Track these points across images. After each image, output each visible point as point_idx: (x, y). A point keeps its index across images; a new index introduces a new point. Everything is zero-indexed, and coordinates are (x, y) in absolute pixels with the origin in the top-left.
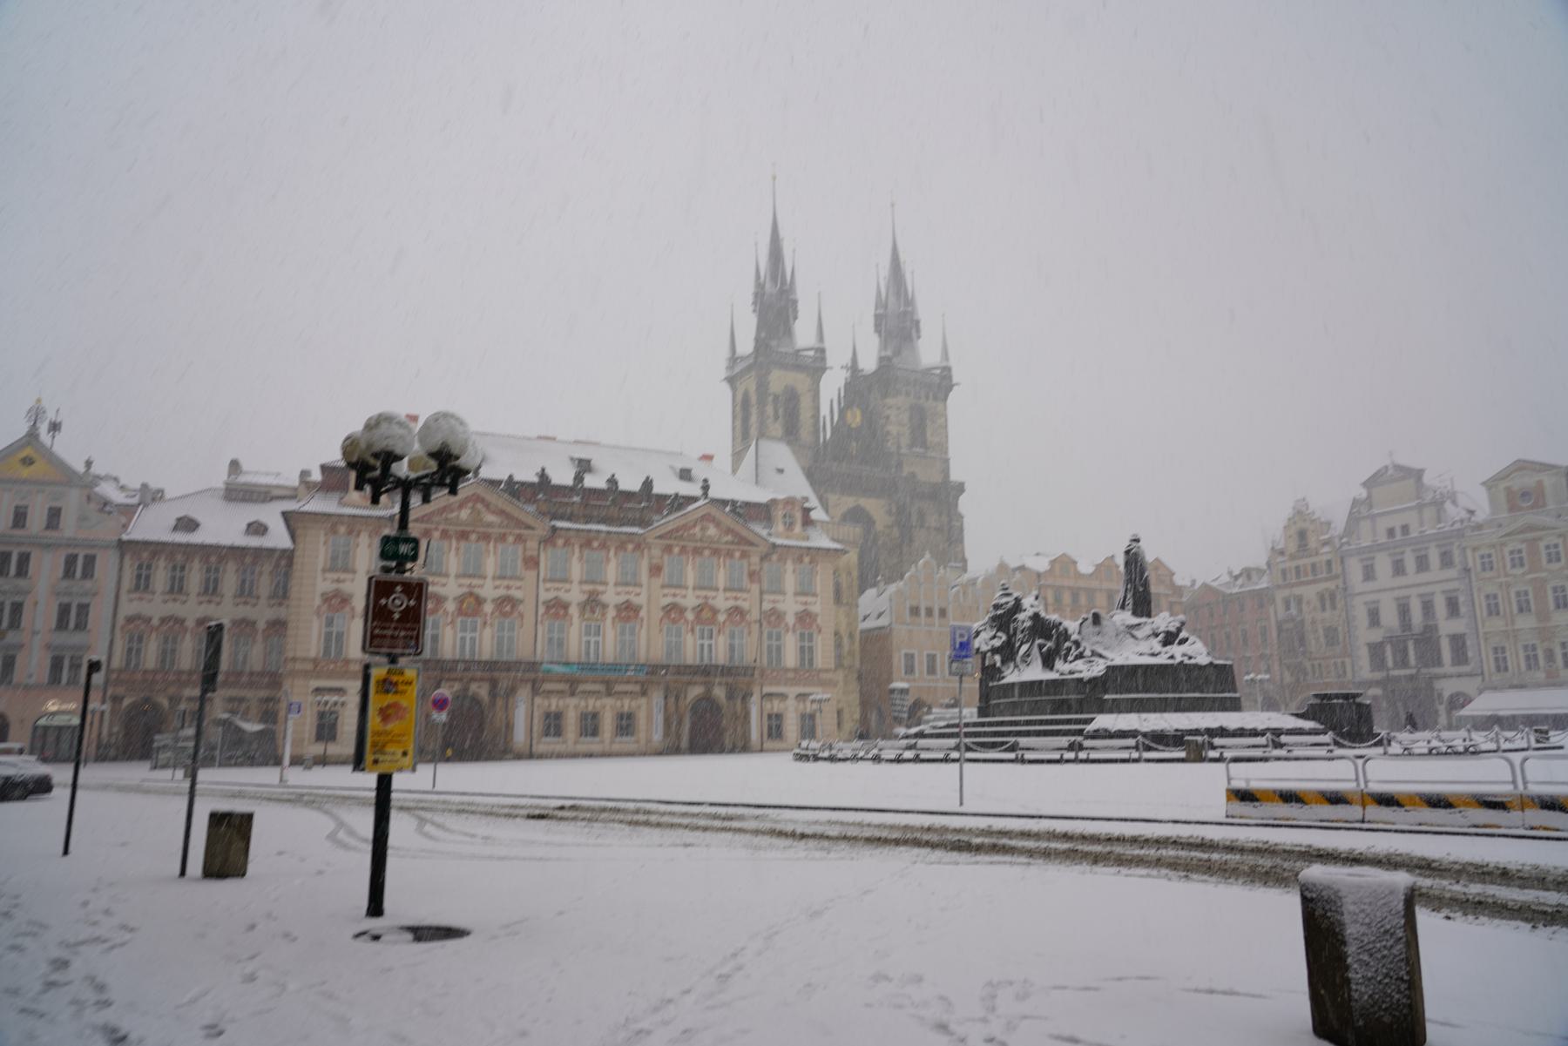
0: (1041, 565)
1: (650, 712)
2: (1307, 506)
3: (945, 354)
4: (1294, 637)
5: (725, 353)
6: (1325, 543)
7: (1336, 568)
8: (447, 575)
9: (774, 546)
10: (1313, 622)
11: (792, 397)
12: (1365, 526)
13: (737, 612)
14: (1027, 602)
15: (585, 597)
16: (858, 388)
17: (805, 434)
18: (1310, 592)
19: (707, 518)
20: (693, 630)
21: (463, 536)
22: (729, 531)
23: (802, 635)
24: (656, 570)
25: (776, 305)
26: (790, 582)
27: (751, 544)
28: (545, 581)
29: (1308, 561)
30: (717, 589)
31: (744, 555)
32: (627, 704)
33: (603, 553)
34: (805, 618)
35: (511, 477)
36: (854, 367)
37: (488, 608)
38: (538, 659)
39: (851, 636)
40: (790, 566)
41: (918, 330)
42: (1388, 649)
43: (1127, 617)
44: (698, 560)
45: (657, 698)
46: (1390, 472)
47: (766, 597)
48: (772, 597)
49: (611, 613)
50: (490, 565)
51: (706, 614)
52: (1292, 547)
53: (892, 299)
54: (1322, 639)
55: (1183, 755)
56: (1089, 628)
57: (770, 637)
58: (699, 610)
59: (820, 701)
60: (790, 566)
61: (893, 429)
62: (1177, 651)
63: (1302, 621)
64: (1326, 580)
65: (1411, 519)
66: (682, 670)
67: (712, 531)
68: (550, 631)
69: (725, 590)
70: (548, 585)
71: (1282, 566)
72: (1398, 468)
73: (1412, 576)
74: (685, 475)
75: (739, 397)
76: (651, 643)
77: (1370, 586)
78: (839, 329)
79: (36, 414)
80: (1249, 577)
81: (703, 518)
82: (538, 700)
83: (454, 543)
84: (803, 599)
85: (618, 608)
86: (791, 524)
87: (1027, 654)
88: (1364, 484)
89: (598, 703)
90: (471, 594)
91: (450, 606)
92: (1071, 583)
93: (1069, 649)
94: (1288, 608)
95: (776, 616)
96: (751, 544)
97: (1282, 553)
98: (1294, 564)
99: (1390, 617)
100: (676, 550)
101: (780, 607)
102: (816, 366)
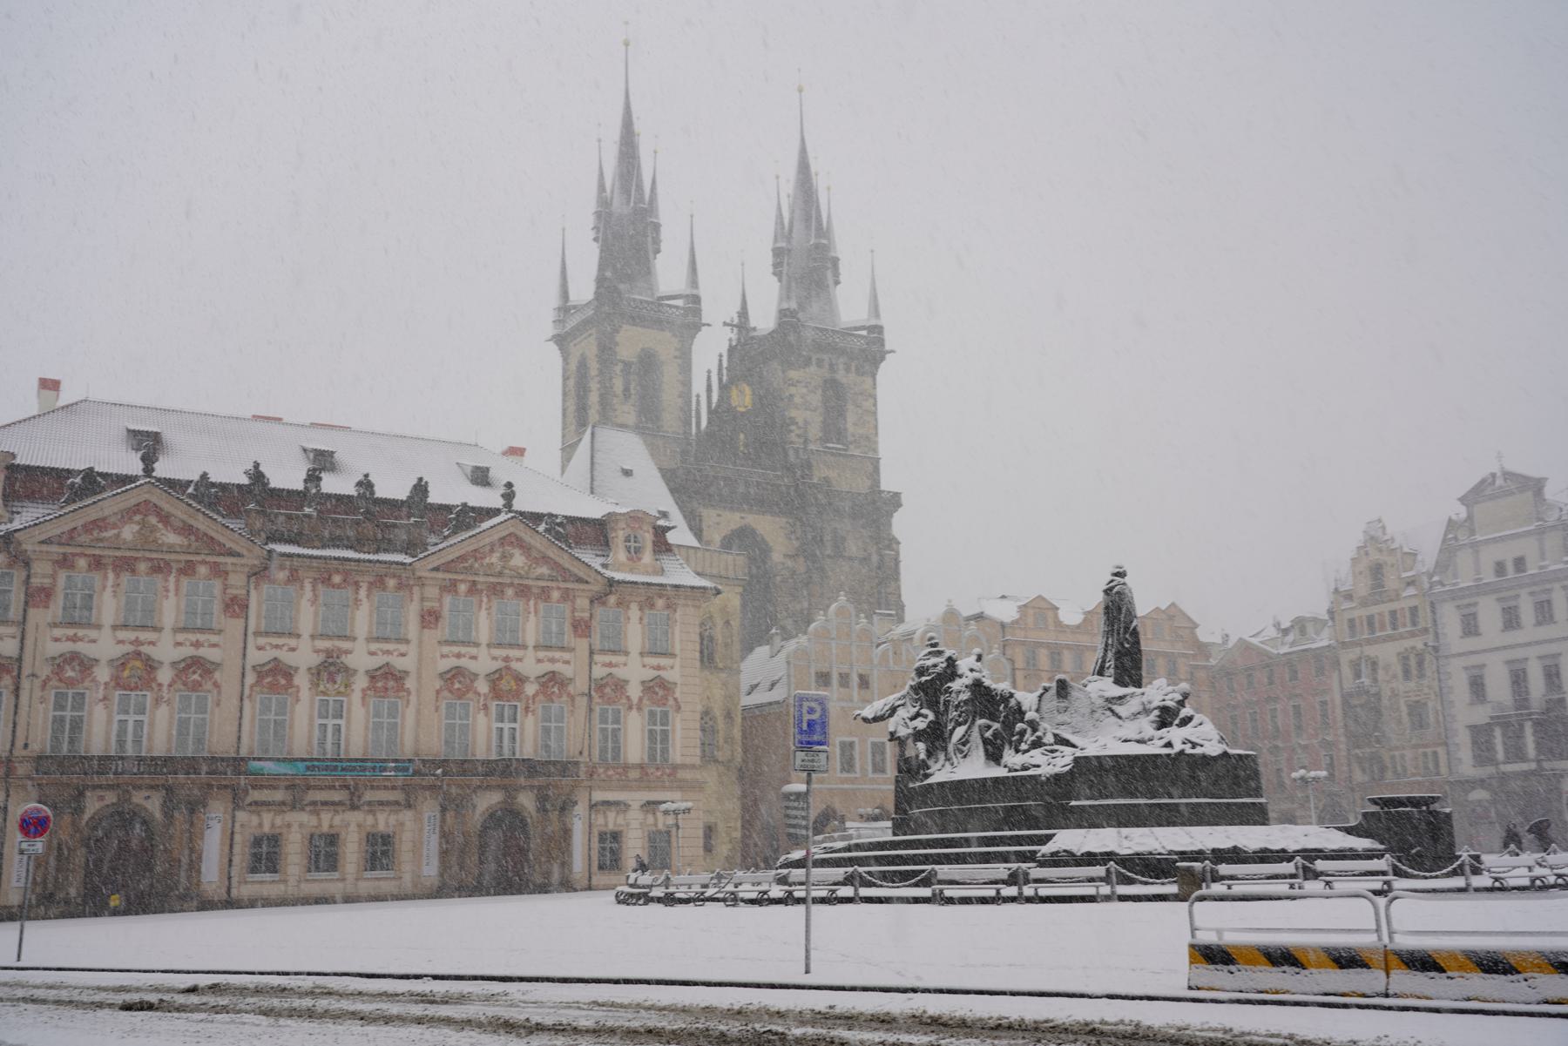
0: (1006, 612)
1: (419, 835)
3: (875, 310)
4: (1365, 713)
5: (554, 301)
6: (1411, 583)
7: (1425, 620)
8: (99, 627)
9: (611, 582)
10: (1394, 694)
11: (648, 363)
12: (1464, 560)
13: (552, 681)
14: (964, 665)
15: (320, 658)
16: (749, 354)
17: (670, 421)
18: (1387, 653)
20: (486, 707)
21: (125, 565)
22: (545, 559)
23: (652, 714)
24: (430, 618)
25: (628, 234)
26: (635, 636)
27: (580, 580)
28: (257, 634)
29: (1385, 608)
30: (525, 647)
31: (567, 596)
32: (383, 822)
33: (349, 592)
34: (658, 688)
35: (204, 476)
36: (742, 323)
37: (165, 675)
38: (244, 753)
39: (729, 716)
40: (634, 612)
41: (836, 274)
42: (1498, 732)
43: (1107, 686)
45: (429, 809)
46: (1499, 482)
47: (597, 658)
48: (608, 658)
49: (361, 682)
50: (169, 612)
51: (505, 685)
52: (1363, 589)
53: (799, 227)
54: (1406, 719)
55: (1173, 889)
56: (1051, 702)
57: (604, 720)
58: (495, 679)
59: (676, 813)
60: (634, 612)
61: (799, 415)
62: (1176, 734)
63: (1378, 695)
64: (1412, 635)
65: (1528, 548)
66: (465, 767)
67: (518, 560)
68: (266, 708)
69: (536, 647)
70: (262, 641)
71: (1347, 616)
72: (1508, 475)
73: (1529, 630)
74: (481, 477)
75: (573, 366)
76: (421, 728)
77: (1471, 643)
78: (724, 270)
80: (1303, 631)
81: (502, 541)
82: (241, 816)
83: (111, 575)
85: (372, 676)
86: (637, 550)
87: (964, 741)
88: (1462, 500)
89: (337, 820)
90: (139, 654)
91: (103, 674)
92: (1049, 637)
93: (1022, 733)
94: (1358, 675)
96: (580, 580)
97: (1349, 596)
98: (1365, 612)
99: (1499, 689)
100: (463, 588)
101: (620, 673)
102: (690, 318)
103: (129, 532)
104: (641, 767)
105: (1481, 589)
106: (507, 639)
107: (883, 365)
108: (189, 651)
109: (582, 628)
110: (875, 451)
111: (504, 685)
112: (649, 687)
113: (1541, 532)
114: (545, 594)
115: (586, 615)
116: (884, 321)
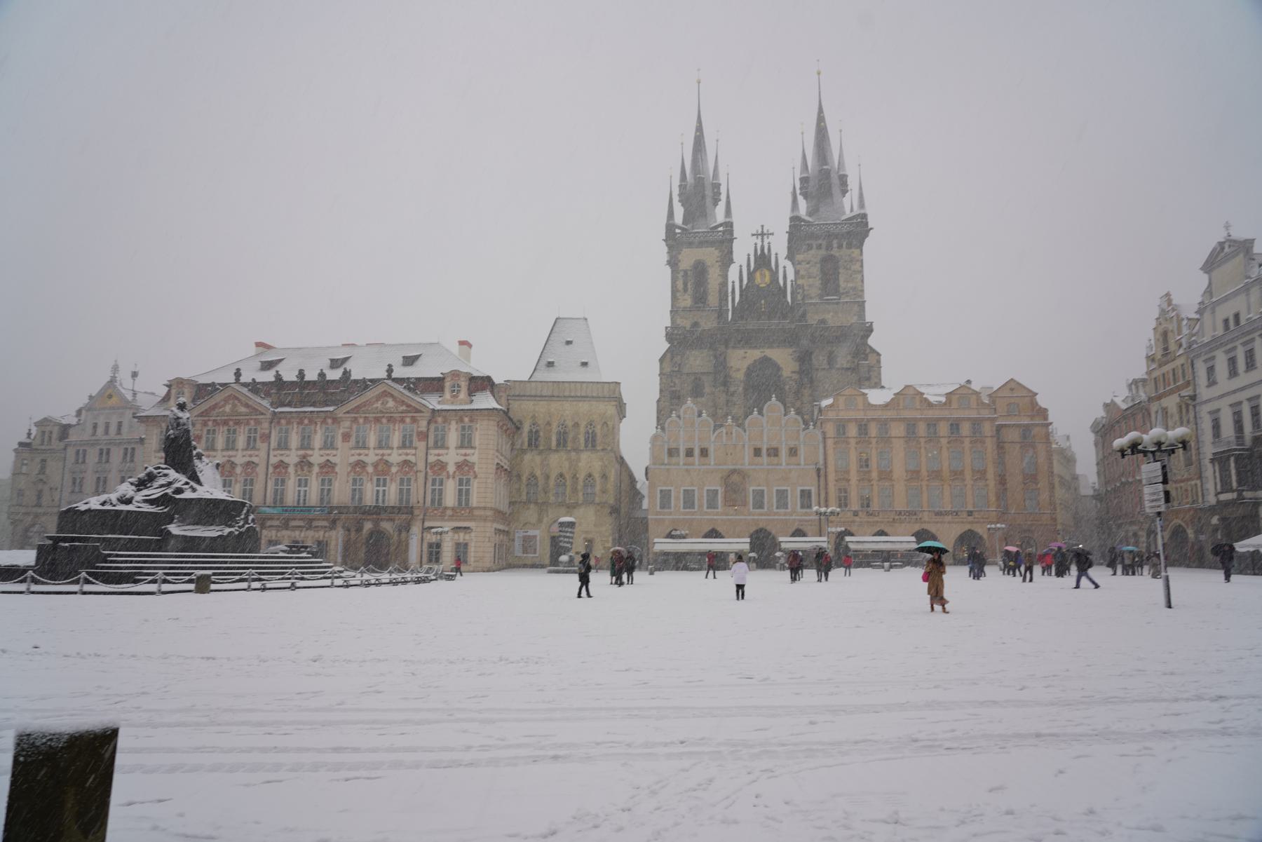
2: (1169, 302)
3: (862, 205)
11: (700, 270)
17: (713, 299)
19: (386, 394)
21: (225, 423)
23: (461, 481)
24: (346, 437)
33: (312, 427)
34: (463, 466)
37: (238, 470)
40: (453, 426)
44: (378, 426)
48: (437, 451)
49: (316, 469)
51: (382, 468)
58: (376, 465)
59: (441, 533)
67: (391, 404)
79: (115, 368)
84: (463, 451)
85: (322, 466)
92: (860, 415)
95: (442, 466)
99: (1228, 430)
100: (361, 421)
103: (228, 408)
104: (453, 509)
105: (1215, 343)
106: (383, 444)
107: (867, 240)
108: (247, 459)
109: (424, 436)
110: (862, 296)
111: (380, 468)
112: (459, 466)
113: (1246, 289)
114: (402, 421)
115: (424, 429)
116: (869, 210)
